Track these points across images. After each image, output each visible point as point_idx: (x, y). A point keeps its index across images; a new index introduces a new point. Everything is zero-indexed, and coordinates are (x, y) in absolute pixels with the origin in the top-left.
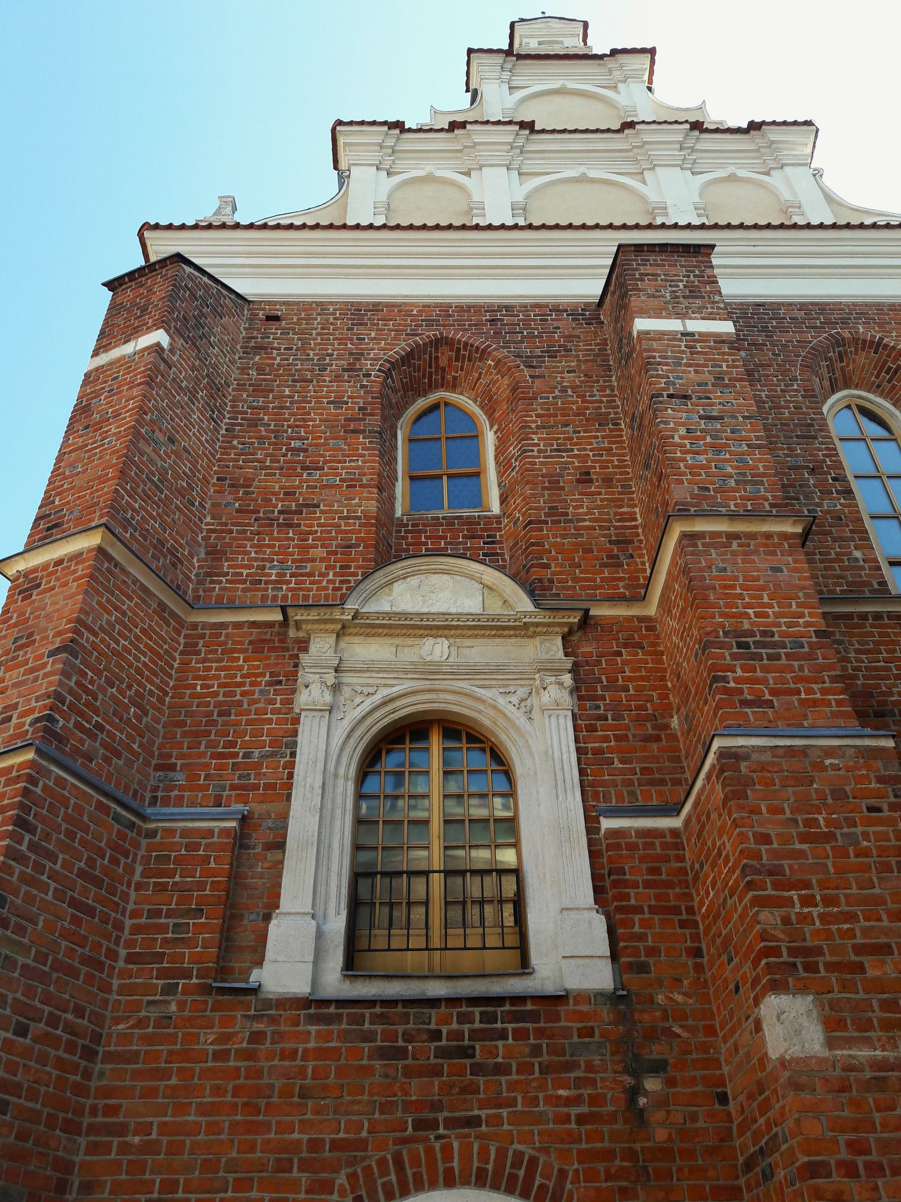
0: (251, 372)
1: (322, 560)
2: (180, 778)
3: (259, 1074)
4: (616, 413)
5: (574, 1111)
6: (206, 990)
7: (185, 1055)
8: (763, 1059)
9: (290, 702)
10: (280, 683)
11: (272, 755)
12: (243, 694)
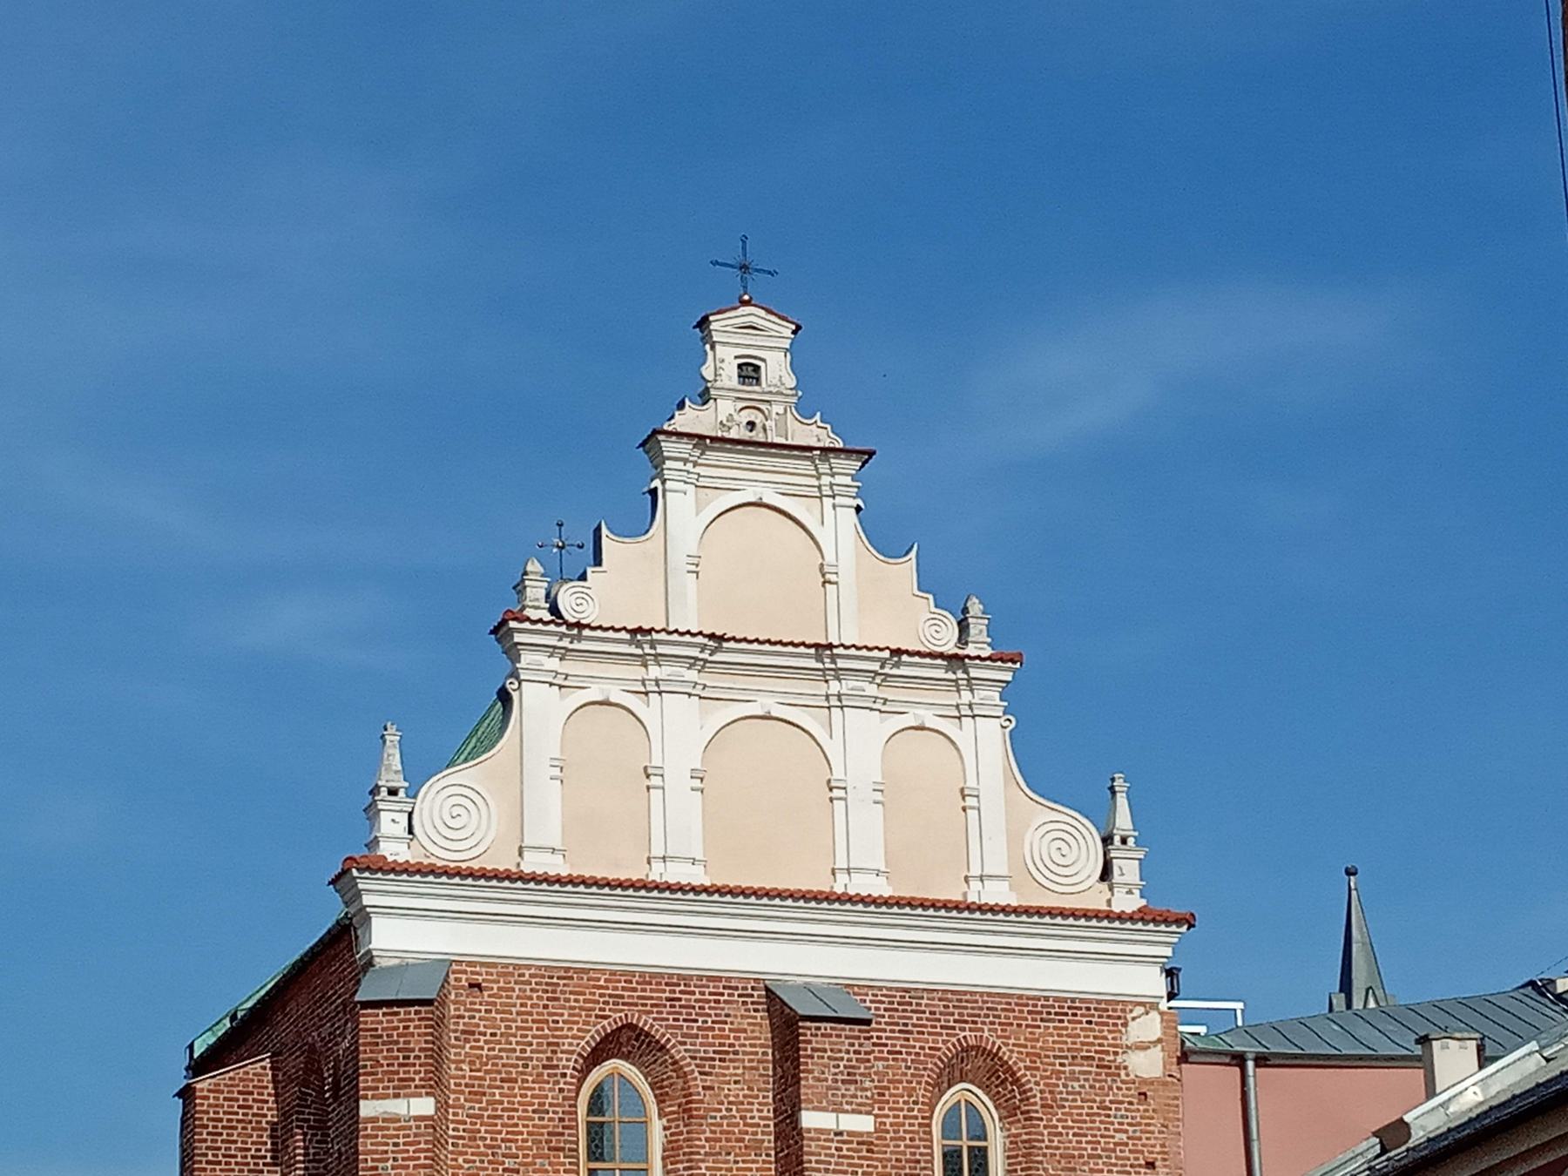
0: (464, 1067)
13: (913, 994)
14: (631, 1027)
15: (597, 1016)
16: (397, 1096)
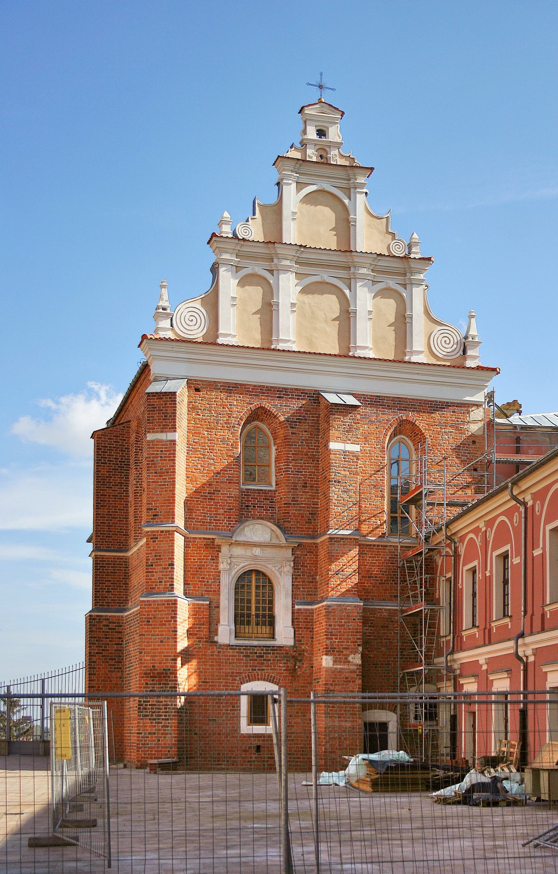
1: (222, 514)
2: (192, 587)
3: (220, 659)
4: (319, 455)
5: (283, 668)
6: (206, 642)
7: (205, 655)
8: (321, 665)
9: (217, 566)
10: (214, 560)
11: (214, 582)
12: (205, 562)
13: (380, 398)
14: (263, 408)
15: (247, 403)
16: (162, 432)
